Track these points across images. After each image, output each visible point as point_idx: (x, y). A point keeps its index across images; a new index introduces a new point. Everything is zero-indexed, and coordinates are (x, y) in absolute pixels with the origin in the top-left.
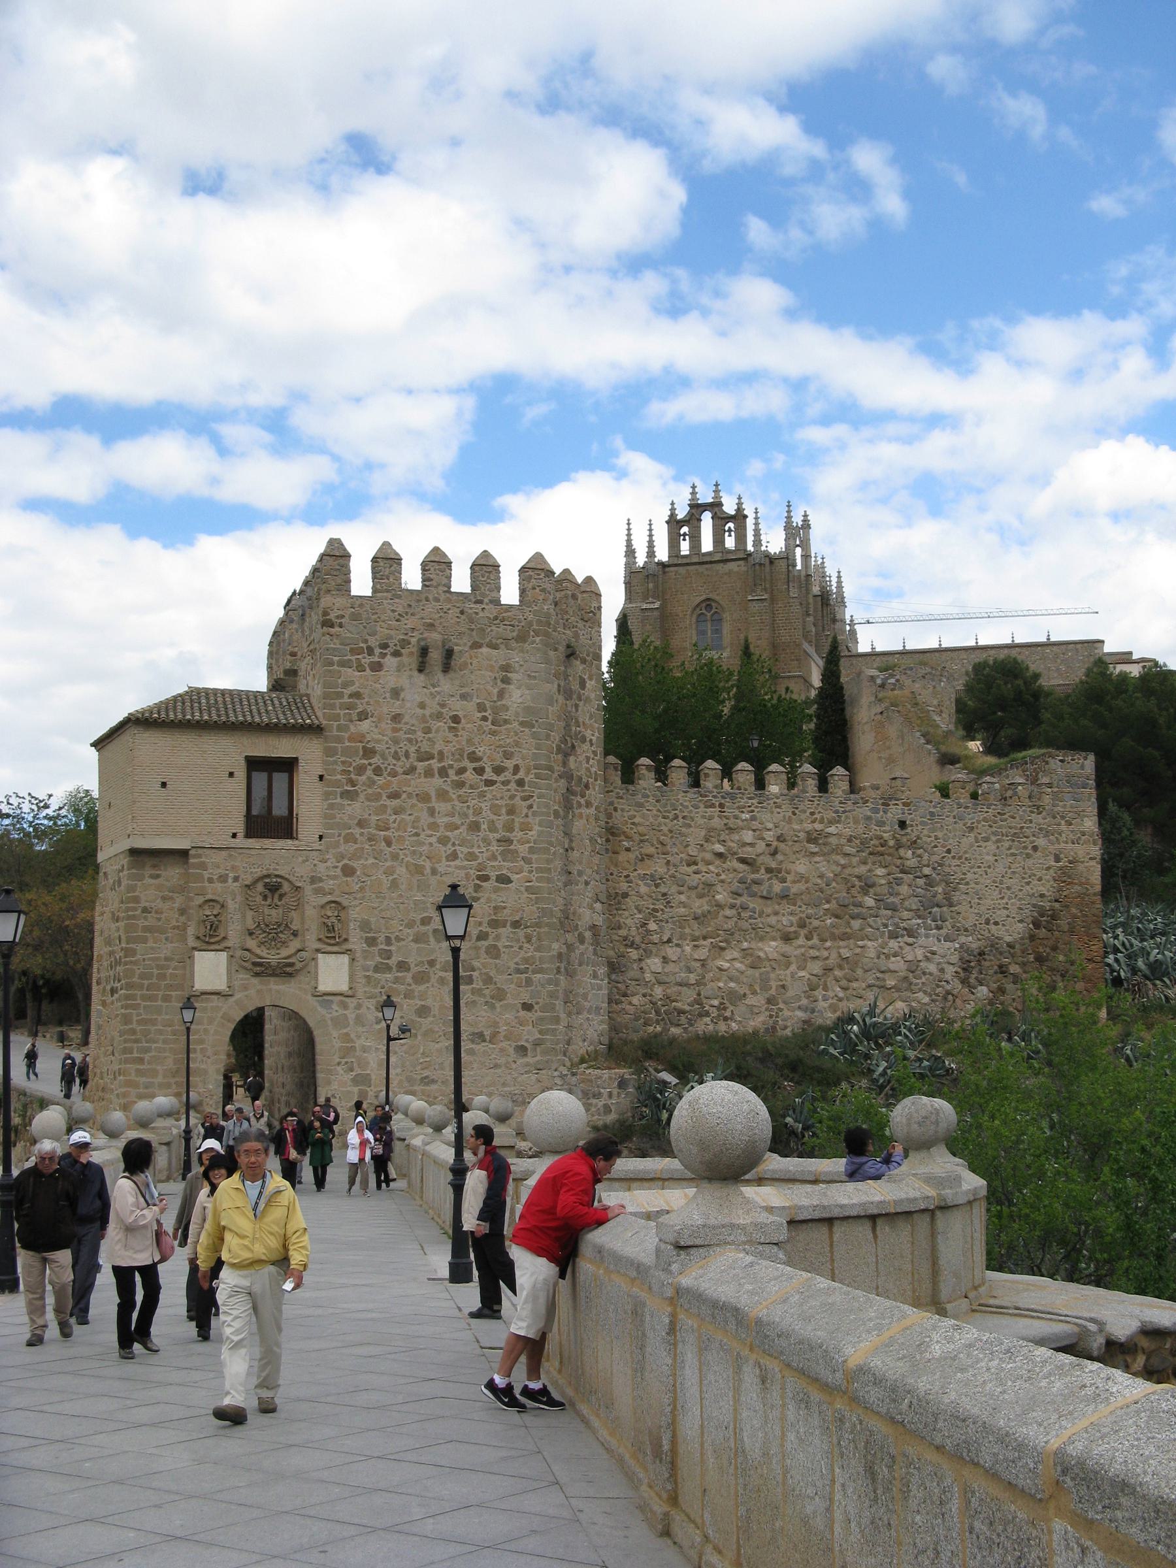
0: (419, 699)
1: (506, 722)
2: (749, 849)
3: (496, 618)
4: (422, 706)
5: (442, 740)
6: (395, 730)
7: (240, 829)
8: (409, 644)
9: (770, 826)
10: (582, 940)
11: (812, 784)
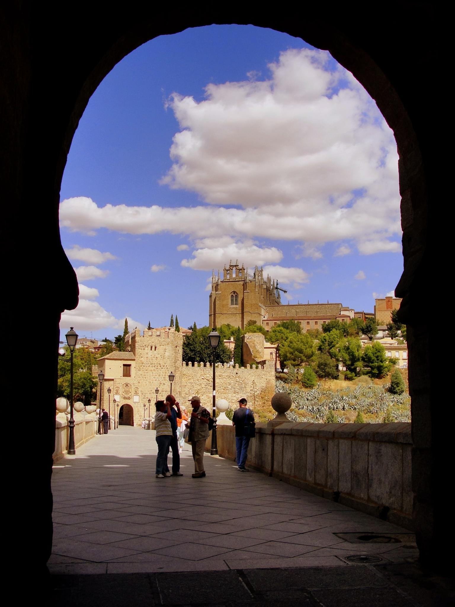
0: (151, 354)
1: (165, 358)
2: (208, 378)
4: (151, 356)
5: (155, 361)
10: (177, 394)
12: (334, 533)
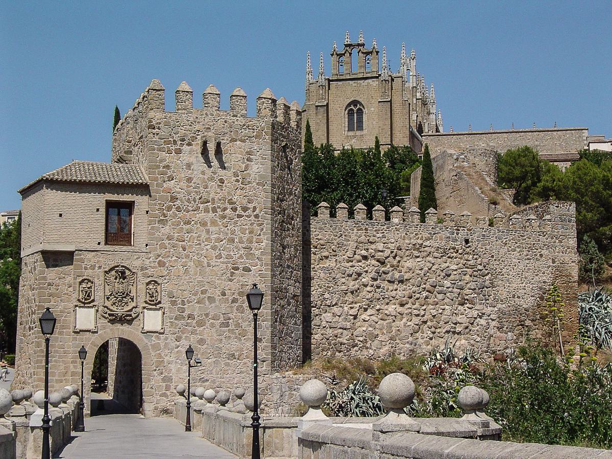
3: (244, 125)
4: (203, 173)
5: (213, 191)
6: (188, 187)
7: (102, 238)
8: (197, 138)
9: (393, 241)
11: (417, 217)
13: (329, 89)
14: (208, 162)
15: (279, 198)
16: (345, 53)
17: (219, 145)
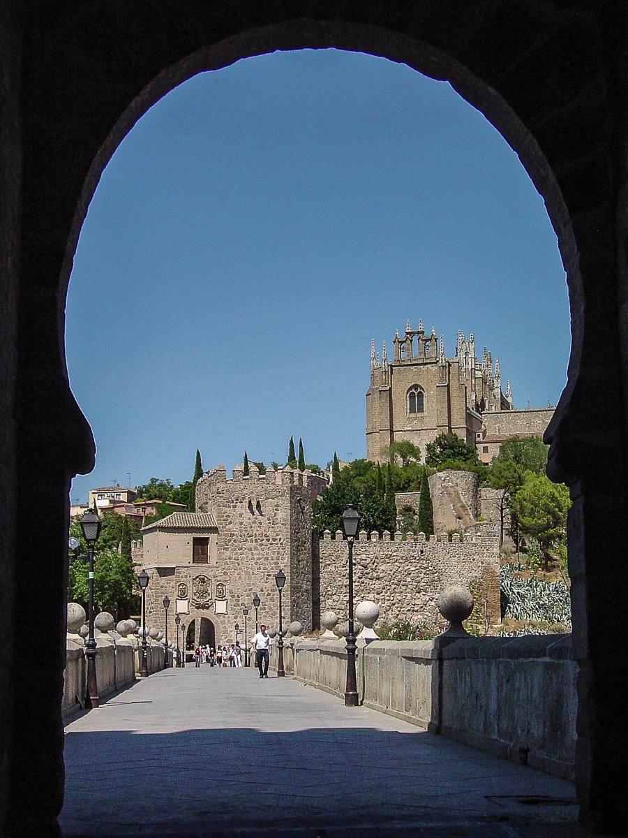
5: (256, 530)
12: (486, 797)
13: (392, 373)
14: (253, 513)
15: (295, 530)
16: (406, 340)
17: (258, 502)
